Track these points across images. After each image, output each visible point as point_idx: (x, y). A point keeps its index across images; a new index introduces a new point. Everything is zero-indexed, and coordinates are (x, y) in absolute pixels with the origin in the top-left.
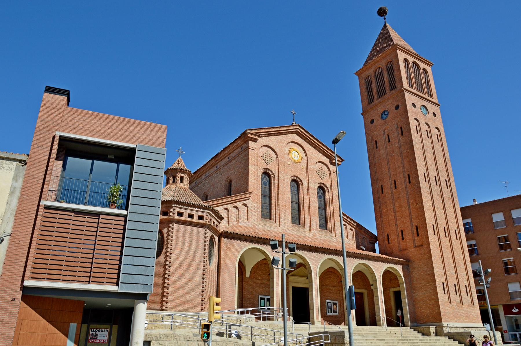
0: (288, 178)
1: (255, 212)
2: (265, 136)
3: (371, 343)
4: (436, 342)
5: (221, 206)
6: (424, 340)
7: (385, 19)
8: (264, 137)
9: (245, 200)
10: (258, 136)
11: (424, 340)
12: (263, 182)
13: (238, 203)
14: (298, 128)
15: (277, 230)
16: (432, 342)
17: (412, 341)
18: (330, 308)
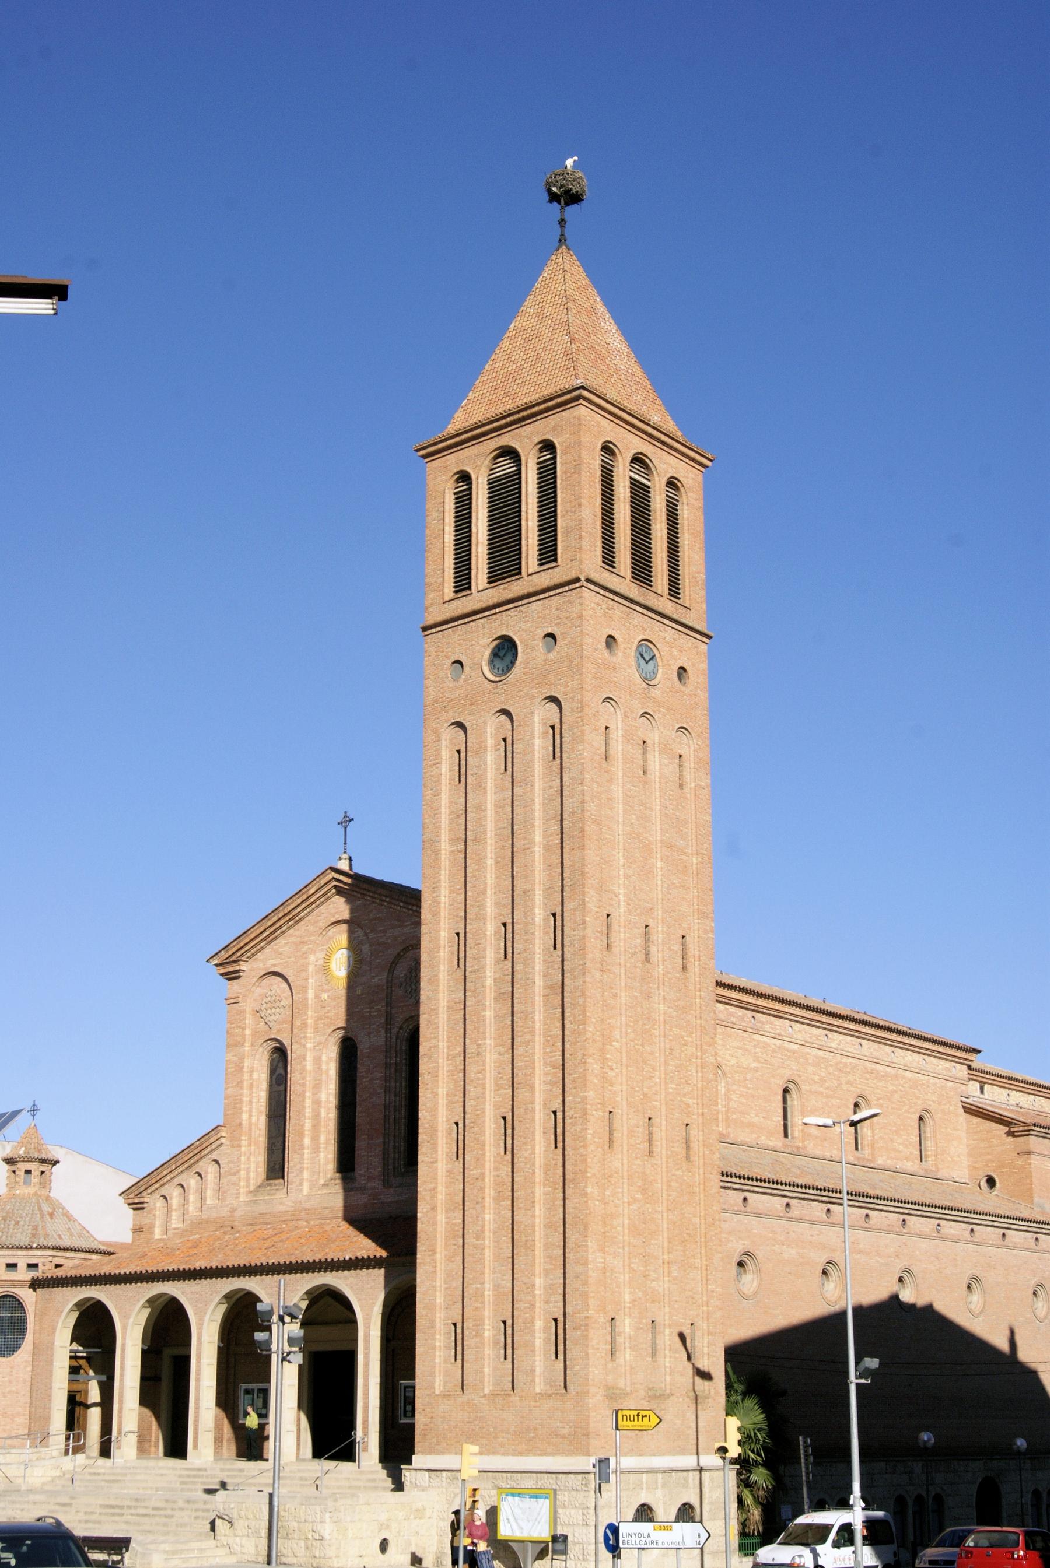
0: (319, 1043)
1: (235, 1174)
2: (263, 948)
3: (22, 1510)
4: (172, 1516)
5: (169, 1181)
6: (165, 1509)
7: (562, 222)
8: (259, 951)
9: (213, 1150)
10: (235, 962)
11: (165, 1509)
12: (274, 1077)
13: (201, 1163)
14: (334, 878)
15: (282, 1208)
16: (160, 1515)
17: (133, 1511)
18: (409, 1404)
